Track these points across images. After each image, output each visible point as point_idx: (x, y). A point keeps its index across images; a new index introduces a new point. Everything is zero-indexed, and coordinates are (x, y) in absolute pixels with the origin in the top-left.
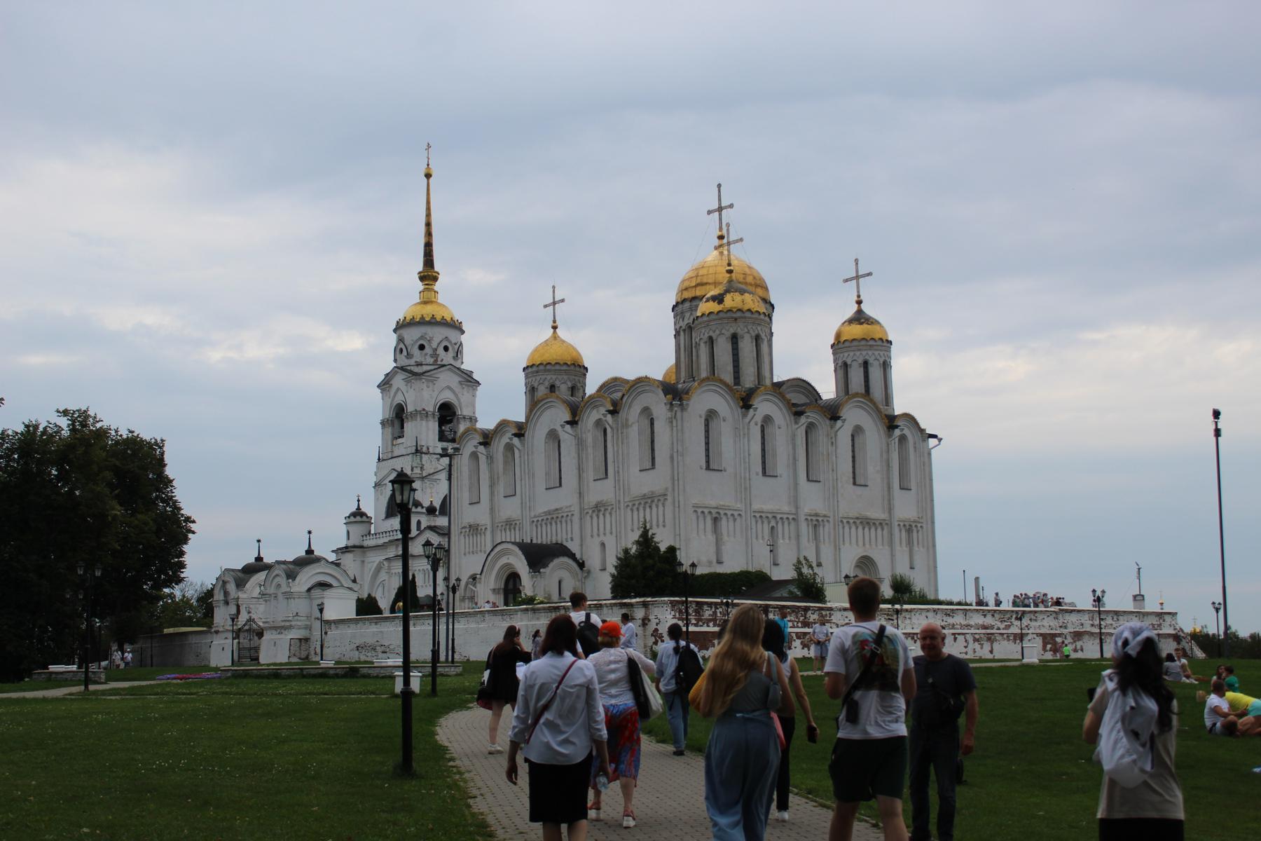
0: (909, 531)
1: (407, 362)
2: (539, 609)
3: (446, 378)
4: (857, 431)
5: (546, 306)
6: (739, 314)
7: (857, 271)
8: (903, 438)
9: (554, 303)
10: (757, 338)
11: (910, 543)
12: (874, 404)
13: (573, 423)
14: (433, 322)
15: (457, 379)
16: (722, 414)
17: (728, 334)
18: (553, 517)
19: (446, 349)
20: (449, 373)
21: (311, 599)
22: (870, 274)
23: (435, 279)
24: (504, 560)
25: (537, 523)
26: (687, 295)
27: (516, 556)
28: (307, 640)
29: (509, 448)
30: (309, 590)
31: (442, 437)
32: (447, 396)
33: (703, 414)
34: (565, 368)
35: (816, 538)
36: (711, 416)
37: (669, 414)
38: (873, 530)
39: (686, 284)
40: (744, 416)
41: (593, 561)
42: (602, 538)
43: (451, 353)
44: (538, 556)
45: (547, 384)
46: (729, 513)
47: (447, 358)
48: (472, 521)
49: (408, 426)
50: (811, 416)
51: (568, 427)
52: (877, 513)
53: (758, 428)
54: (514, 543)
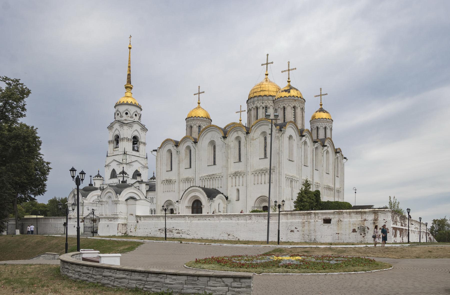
1: (120, 119)
2: (295, 214)
3: (136, 127)
5: (195, 94)
6: (296, 98)
7: (321, 93)
9: (199, 93)
10: (302, 108)
13: (225, 137)
14: (131, 104)
17: (292, 106)
18: (211, 177)
19: (136, 115)
20: (137, 125)
21: (127, 205)
22: (326, 94)
24: (193, 194)
25: (202, 179)
26: (255, 94)
27: (200, 192)
28: (126, 225)
29: (188, 147)
30: (126, 200)
31: (134, 149)
32: (136, 134)
34: (205, 119)
36: (290, 137)
39: (255, 90)
40: (301, 139)
41: (233, 196)
42: (237, 187)
43: (138, 117)
44: (211, 194)
45: (197, 125)
47: (136, 119)
48: (168, 178)
49: (120, 144)
54: (199, 187)
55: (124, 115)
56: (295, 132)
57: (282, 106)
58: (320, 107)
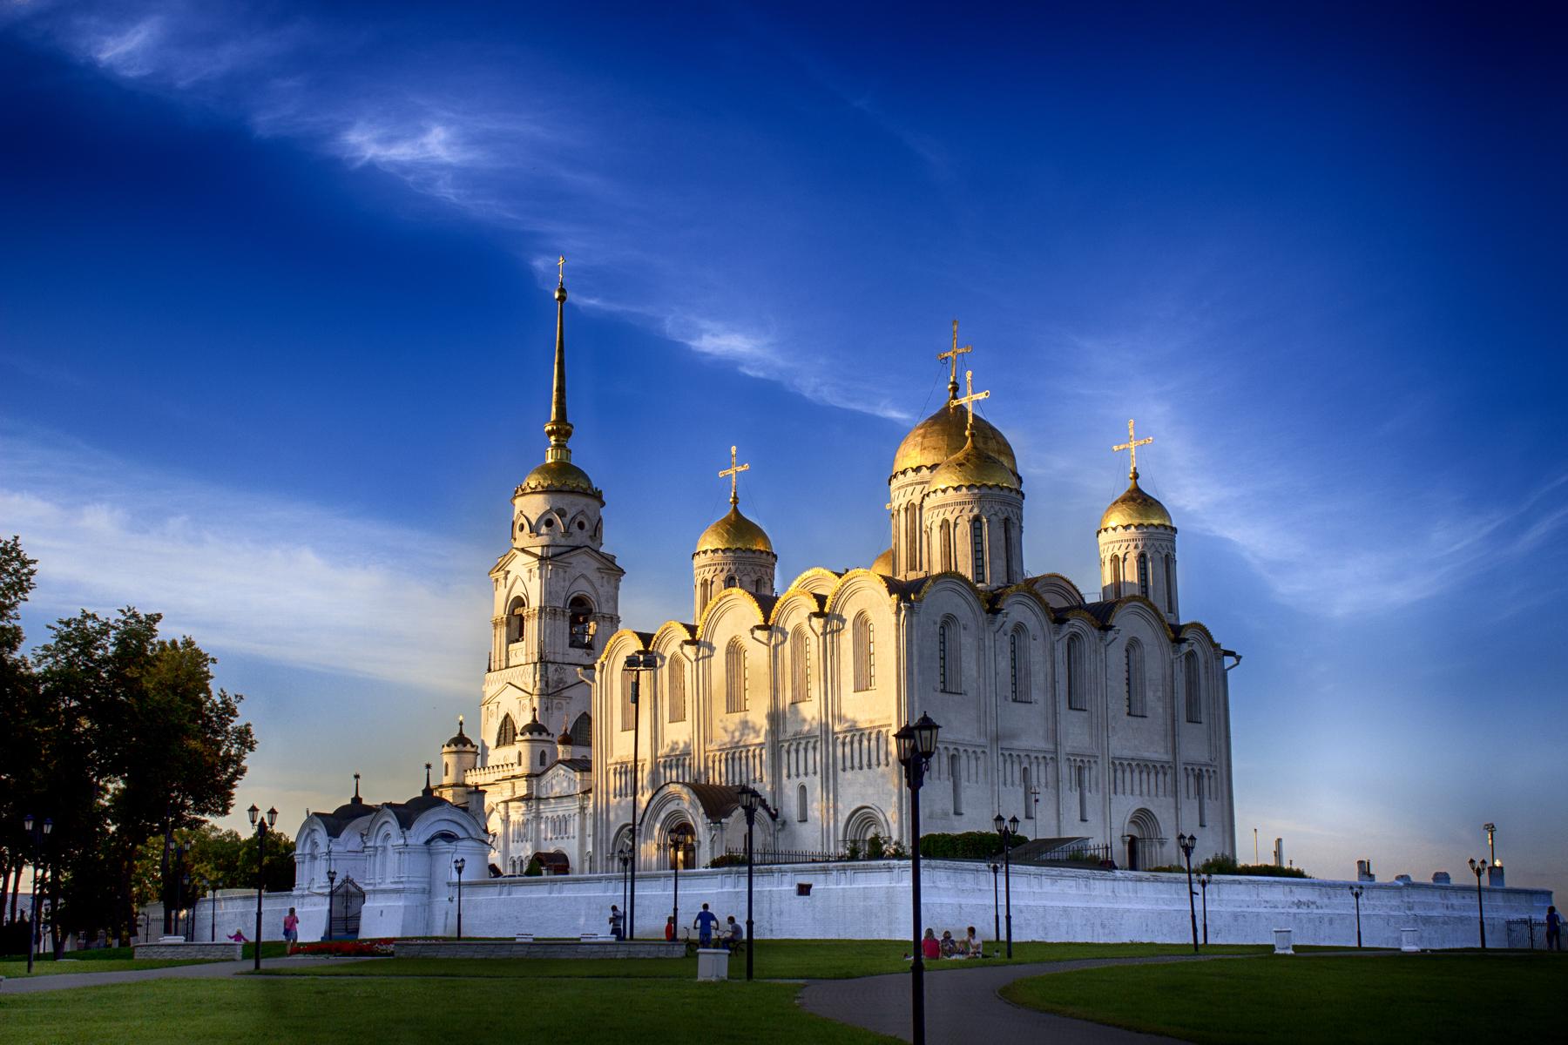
0: (1199, 777)
3: (583, 564)
4: (1133, 645)
8: (1191, 655)
11: (1200, 793)
12: (1155, 610)
15: (597, 565)
16: (962, 622)
19: (581, 526)
20: (585, 558)
21: (430, 853)
23: (568, 434)
24: (671, 807)
30: (428, 842)
31: (575, 642)
32: (582, 588)
33: (939, 620)
35: (1080, 783)
36: (948, 621)
37: (893, 619)
38: (1152, 775)
40: (992, 622)
44: (716, 802)
46: (970, 750)
47: (580, 537)
50: (1076, 624)
51: (758, 633)
52: (1158, 753)
53: (1007, 639)
54: (684, 784)
55: (544, 529)
56: (968, 603)
57: (941, 517)
58: (1130, 484)
